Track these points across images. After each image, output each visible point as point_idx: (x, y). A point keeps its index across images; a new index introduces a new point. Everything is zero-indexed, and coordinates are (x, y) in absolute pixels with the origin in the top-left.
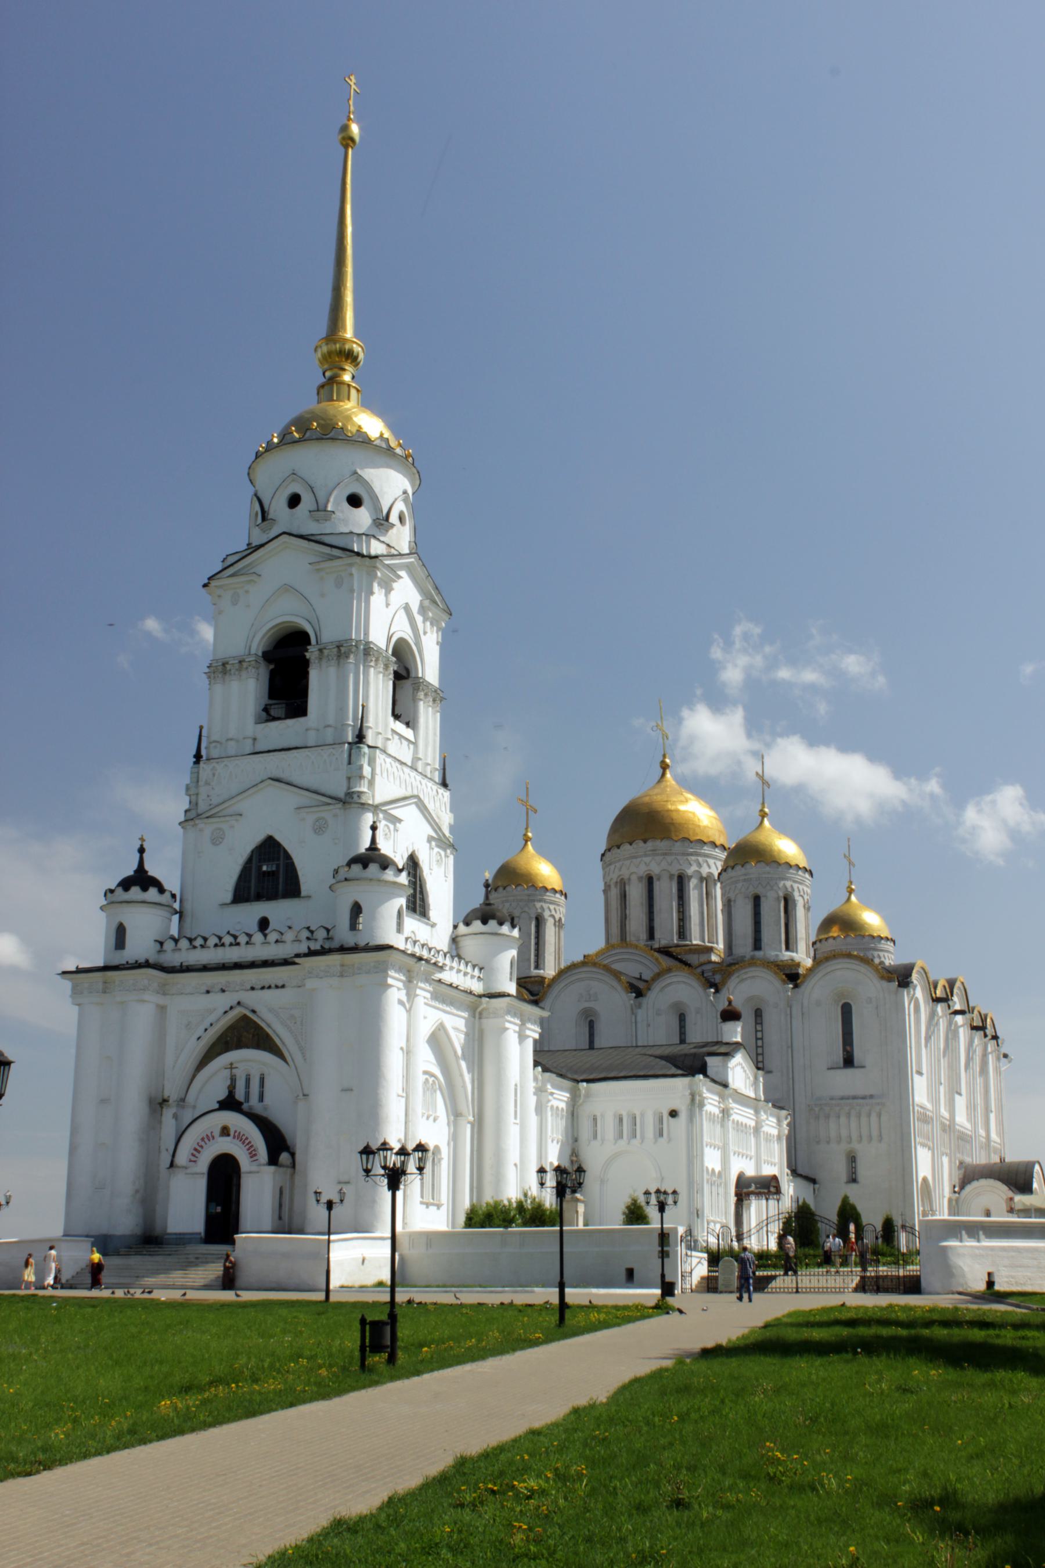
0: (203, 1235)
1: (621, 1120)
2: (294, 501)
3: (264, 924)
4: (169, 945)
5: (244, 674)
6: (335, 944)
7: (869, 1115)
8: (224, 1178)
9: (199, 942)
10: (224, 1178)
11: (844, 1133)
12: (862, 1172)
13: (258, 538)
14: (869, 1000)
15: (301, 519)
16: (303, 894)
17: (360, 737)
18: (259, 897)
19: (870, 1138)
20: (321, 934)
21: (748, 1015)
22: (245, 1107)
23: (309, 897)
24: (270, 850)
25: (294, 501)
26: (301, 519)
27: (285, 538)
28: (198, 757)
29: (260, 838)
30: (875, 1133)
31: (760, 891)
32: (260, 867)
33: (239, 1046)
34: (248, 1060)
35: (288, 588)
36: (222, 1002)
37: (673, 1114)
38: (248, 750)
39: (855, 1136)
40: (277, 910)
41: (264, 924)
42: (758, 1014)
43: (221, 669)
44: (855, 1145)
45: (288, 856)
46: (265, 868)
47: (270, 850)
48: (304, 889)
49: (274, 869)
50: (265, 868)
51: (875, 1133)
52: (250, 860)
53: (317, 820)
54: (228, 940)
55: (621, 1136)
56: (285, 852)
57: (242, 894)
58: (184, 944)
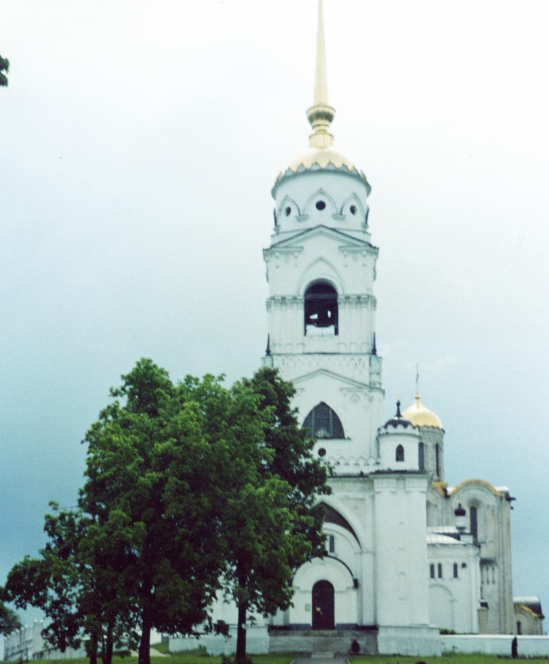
2: (321, 206)
5: (295, 306)
6: (380, 468)
7: (487, 569)
13: (289, 224)
14: (488, 506)
15: (325, 217)
17: (374, 352)
19: (488, 582)
20: (372, 462)
21: (468, 513)
22: (330, 554)
23: (349, 439)
25: (321, 206)
26: (325, 217)
27: (322, 229)
28: (268, 352)
29: (317, 403)
30: (491, 579)
35: (321, 259)
37: (464, 565)
38: (301, 351)
42: (474, 511)
43: (278, 301)
48: (347, 435)
51: (491, 581)
52: (310, 414)
53: (353, 396)
56: (333, 412)
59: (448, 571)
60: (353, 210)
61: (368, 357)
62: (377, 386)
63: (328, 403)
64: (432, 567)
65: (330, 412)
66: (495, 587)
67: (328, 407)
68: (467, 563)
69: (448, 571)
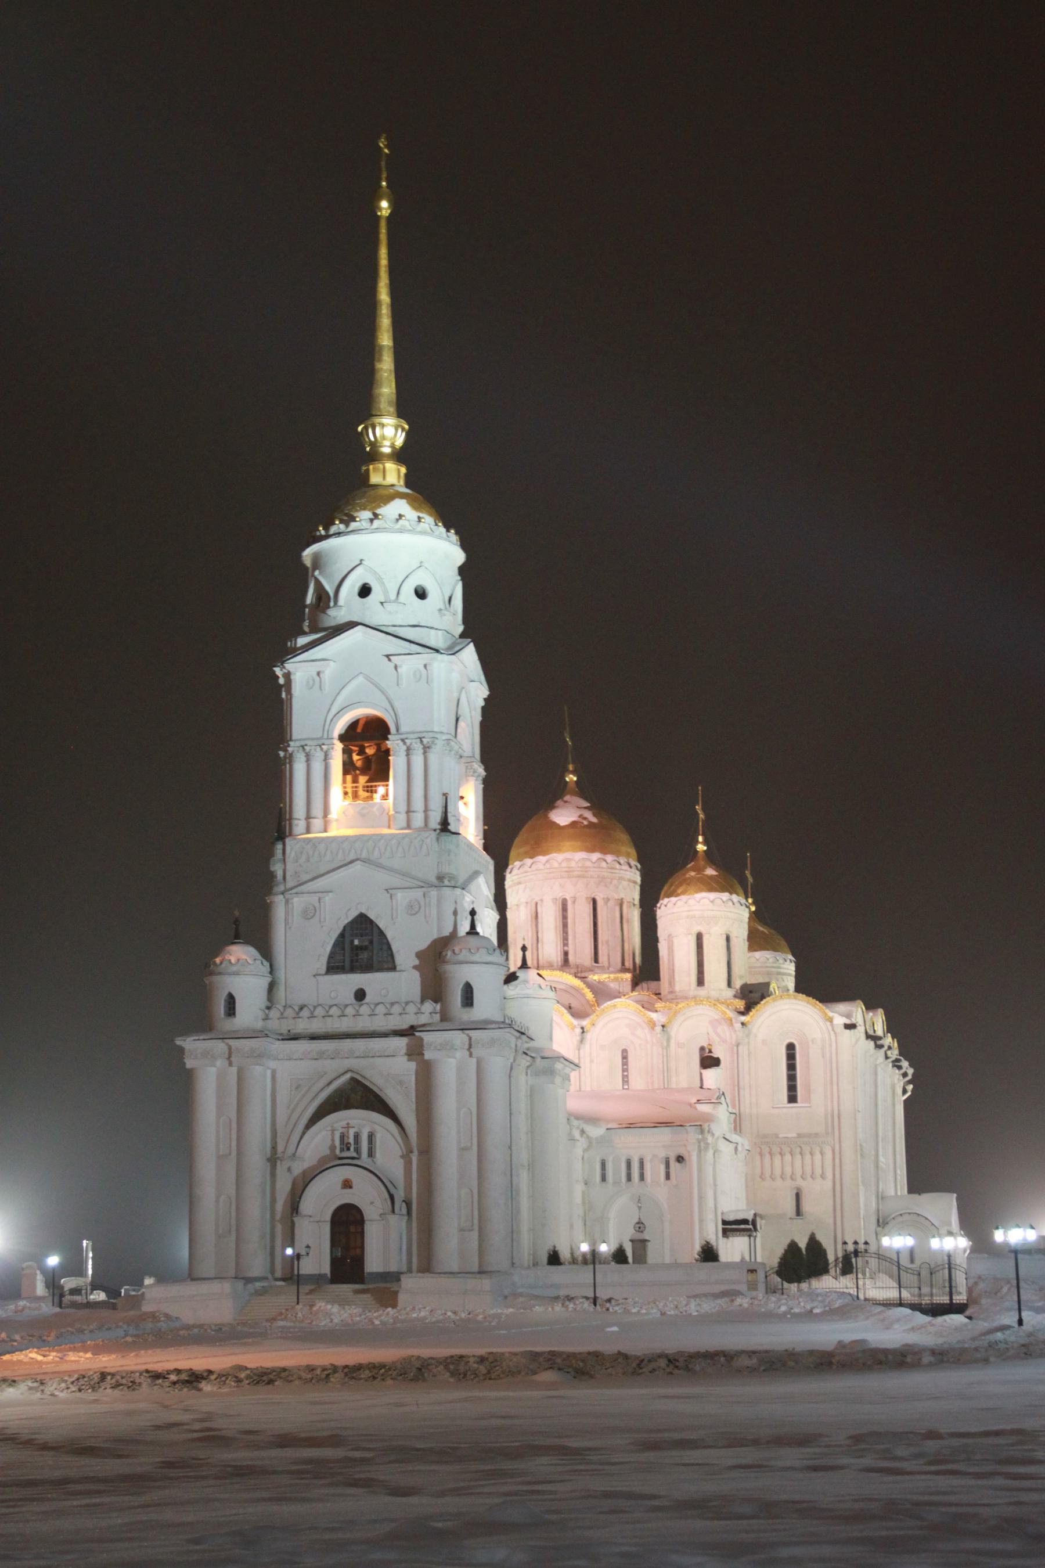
0: (329, 1275)
1: (629, 1164)
3: (360, 995)
4: (274, 1014)
8: (347, 1223)
9: (305, 1013)
10: (347, 1223)
11: (788, 1171)
12: (806, 1206)
16: (398, 968)
18: (352, 970)
24: (363, 924)
31: (703, 931)
32: (352, 942)
33: (348, 1107)
34: (359, 1120)
36: (333, 1067)
39: (798, 1172)
40: (372, 981)
41: (360, 995)
44: (800, 1182)
45: (381, 933)
46: (356, 942)
47: (363, 924)
49: (366, 943)
50: (356, 942)
52: (342, 935)
54: (334, 1011)
55: (629, 1178)
57: (335, 966)
58: (289, 1012)
59: (655, 1171)
60: (421, 594)
61: (434, 835)
62: (453, 883)
63: (372, 916)
64: (629, 1164)
65: (375, 929)
66: (829, 1183)
67: (371, 922)
68: (686, 1157)
69: (655, 1171)
